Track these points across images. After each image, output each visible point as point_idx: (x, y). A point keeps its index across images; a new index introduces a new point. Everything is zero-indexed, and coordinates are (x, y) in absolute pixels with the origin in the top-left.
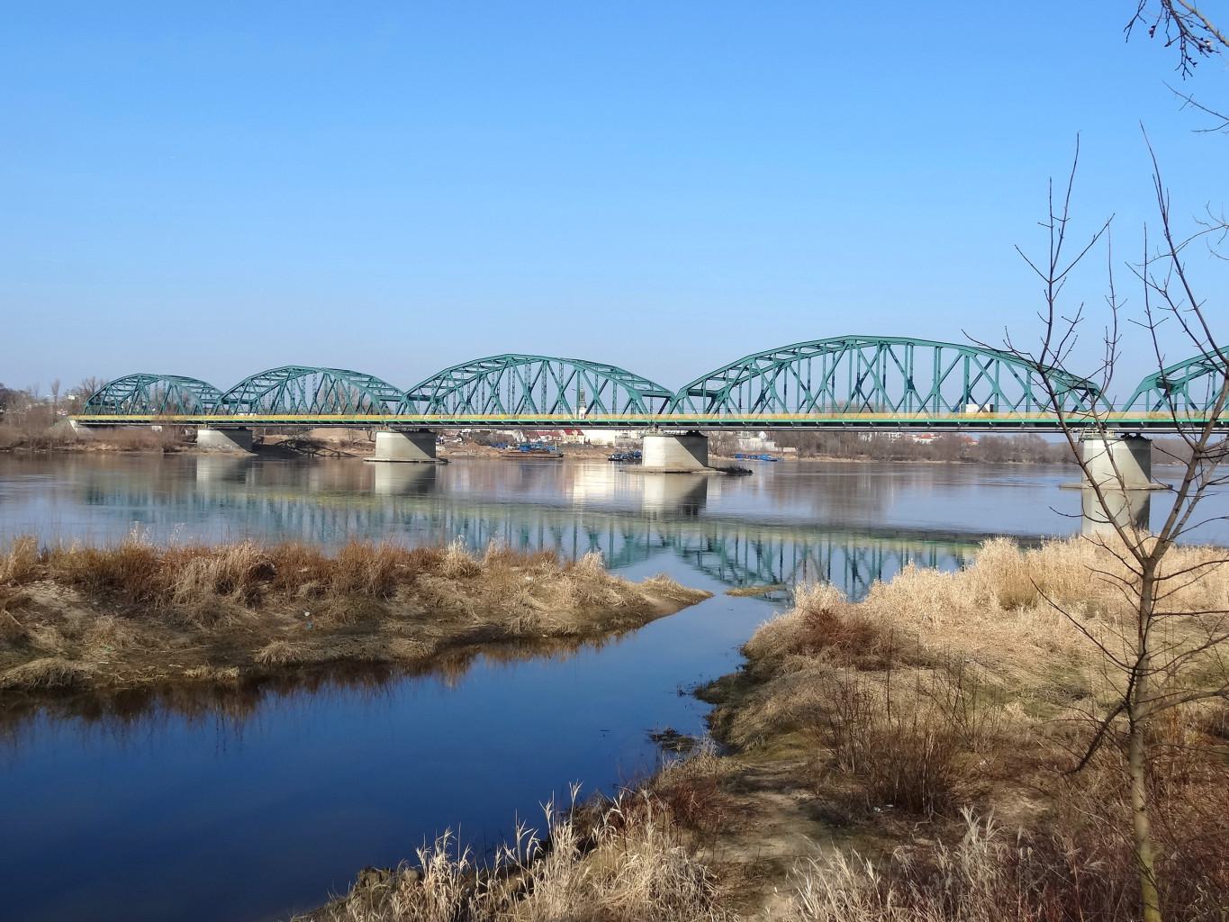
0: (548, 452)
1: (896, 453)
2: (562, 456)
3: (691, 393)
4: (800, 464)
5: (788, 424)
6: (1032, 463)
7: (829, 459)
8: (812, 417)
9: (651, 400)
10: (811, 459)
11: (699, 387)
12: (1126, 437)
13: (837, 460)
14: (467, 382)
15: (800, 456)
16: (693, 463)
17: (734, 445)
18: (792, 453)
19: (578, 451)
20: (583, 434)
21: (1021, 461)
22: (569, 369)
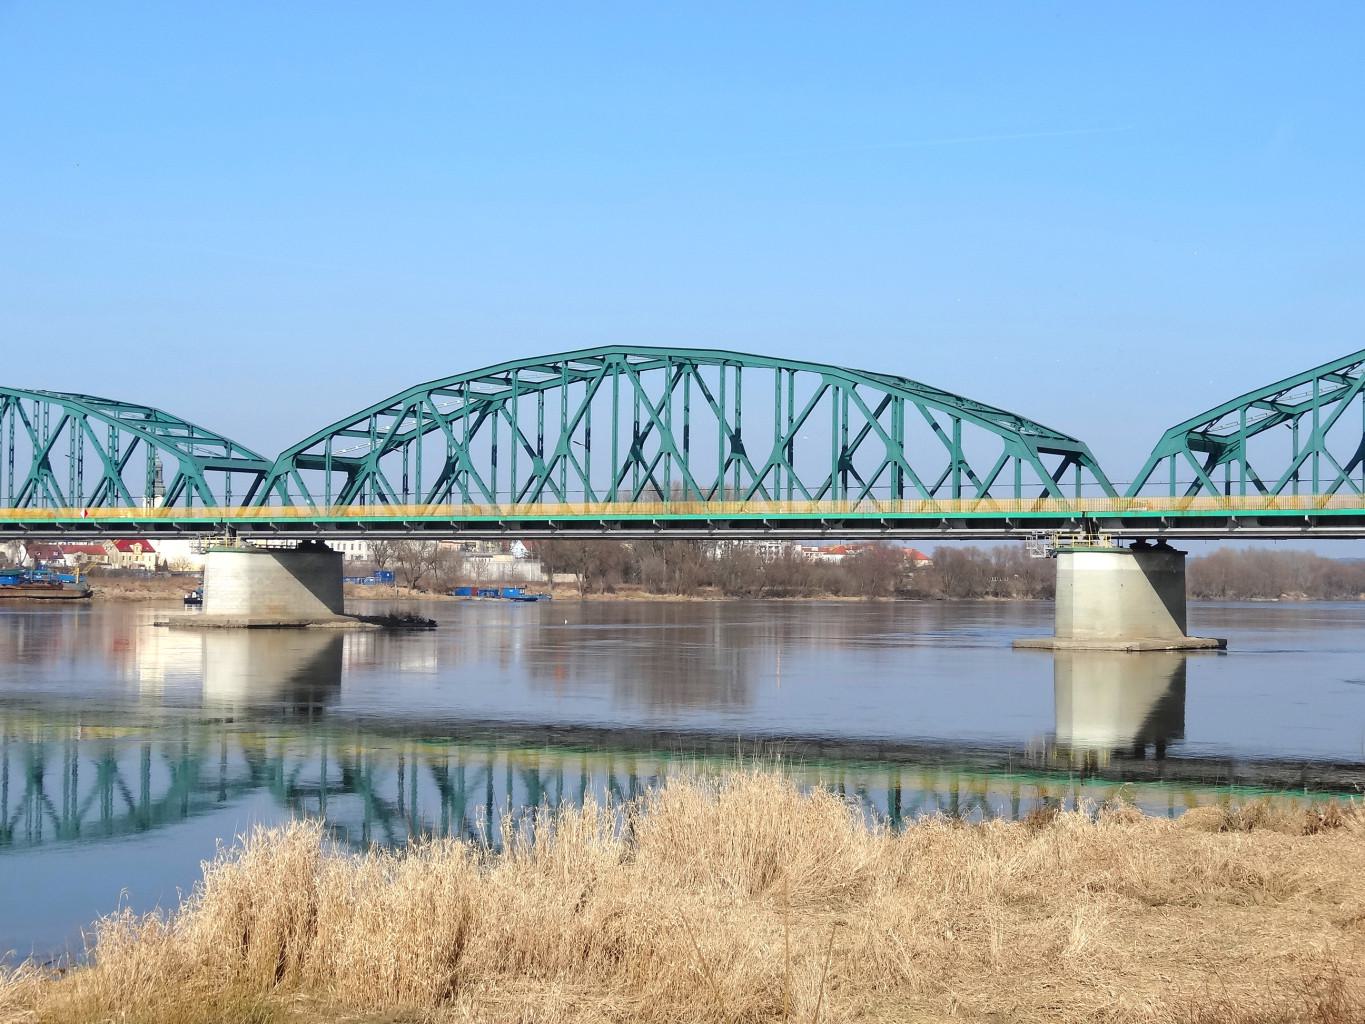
0: (60, 587)
1: (773, 582)
2: (88, 595)
3: (301, 461)
4: (585, 604)
5: (594, 524)
6: (1030, 598)
7: (644, 596)
8: (645, 510)
9: (228, 478)
10: (608, 597)
11: (318, 450)
12: (1139, 548)
13: (659, 598)
15: (585, 590)
16: (308, 604)
17: (453, 569)
18: (570, 585)
19: (129, 585)
20: (152, 550)
21: (1008, 594)
22: (57, 411)
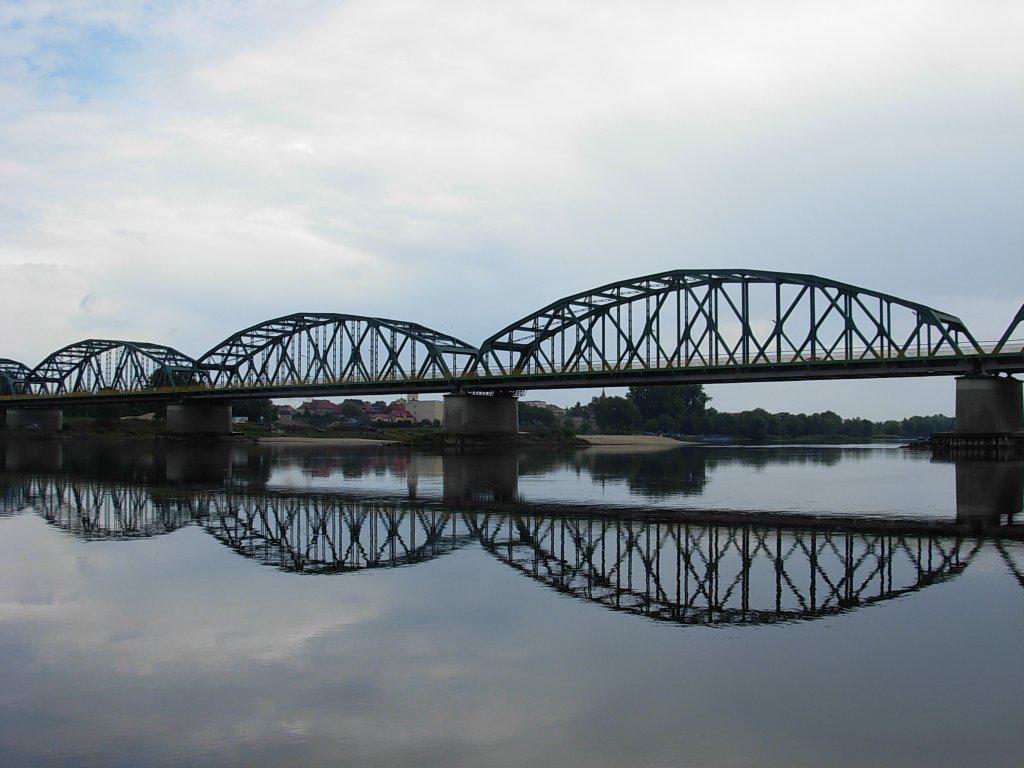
11: (504, 339)
14: (260, 348)
